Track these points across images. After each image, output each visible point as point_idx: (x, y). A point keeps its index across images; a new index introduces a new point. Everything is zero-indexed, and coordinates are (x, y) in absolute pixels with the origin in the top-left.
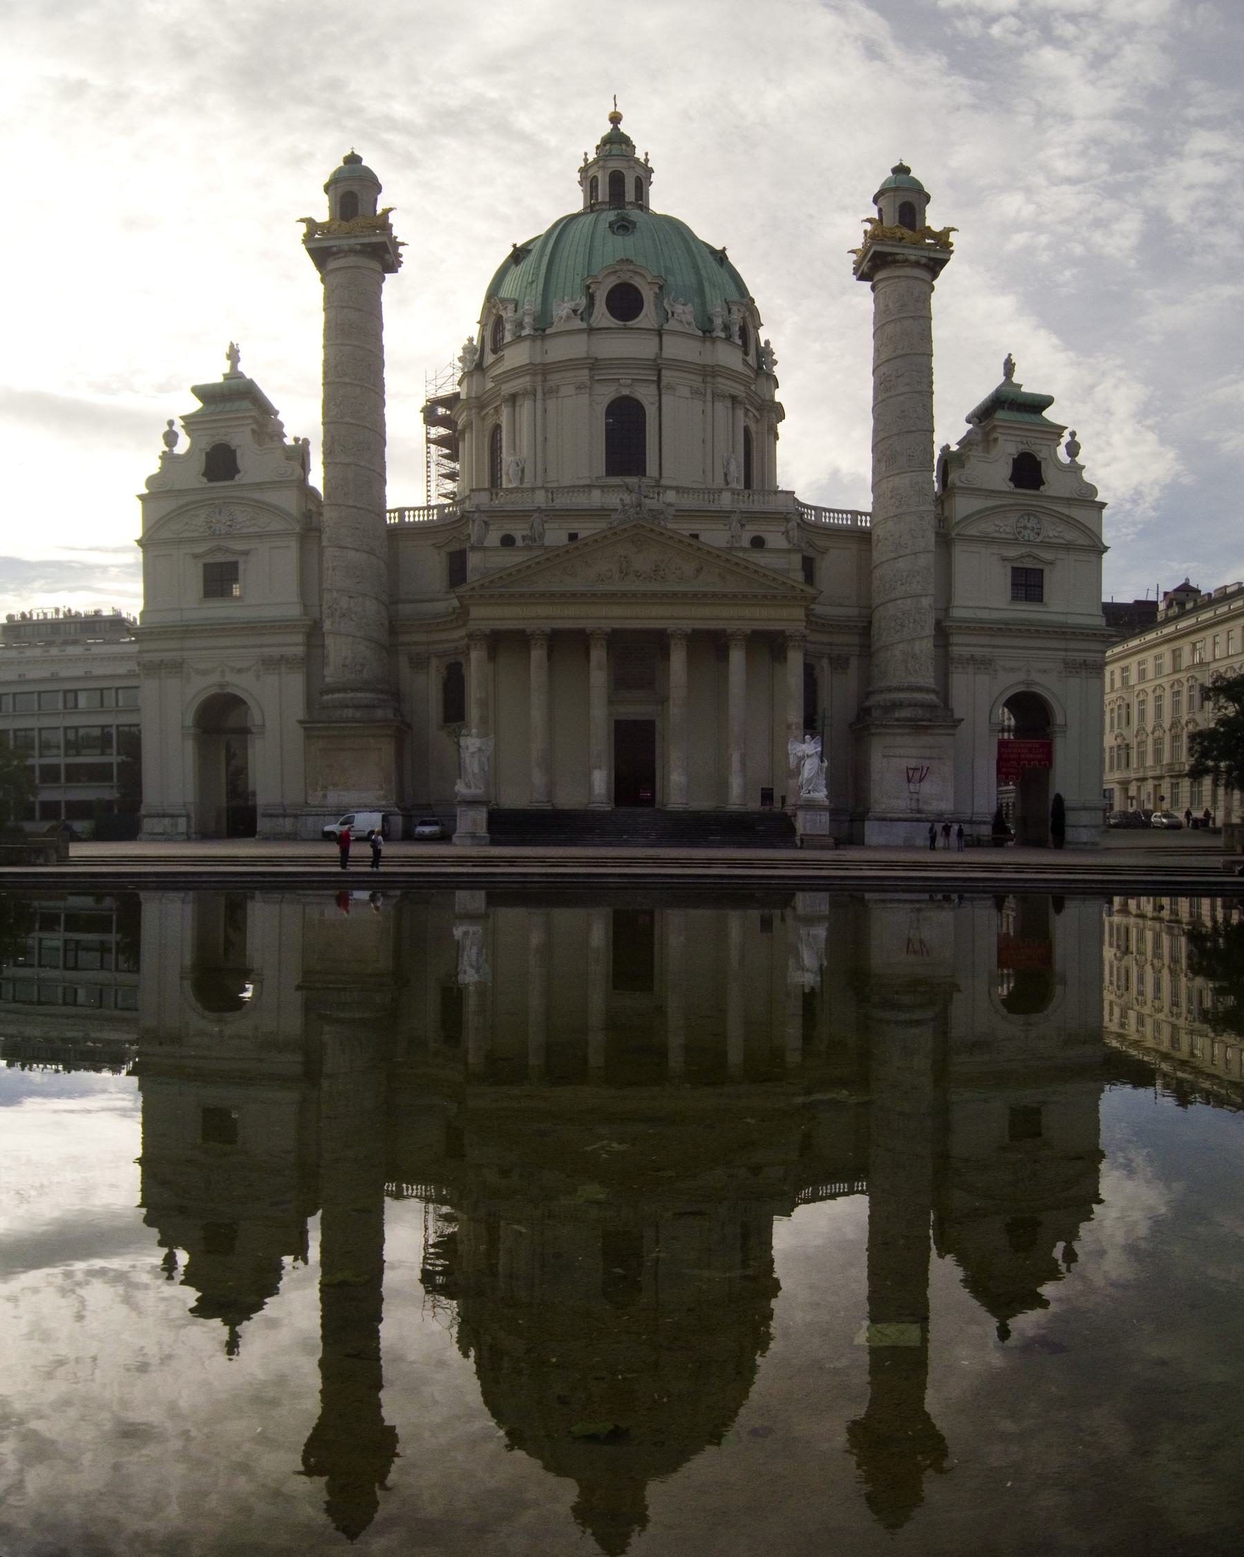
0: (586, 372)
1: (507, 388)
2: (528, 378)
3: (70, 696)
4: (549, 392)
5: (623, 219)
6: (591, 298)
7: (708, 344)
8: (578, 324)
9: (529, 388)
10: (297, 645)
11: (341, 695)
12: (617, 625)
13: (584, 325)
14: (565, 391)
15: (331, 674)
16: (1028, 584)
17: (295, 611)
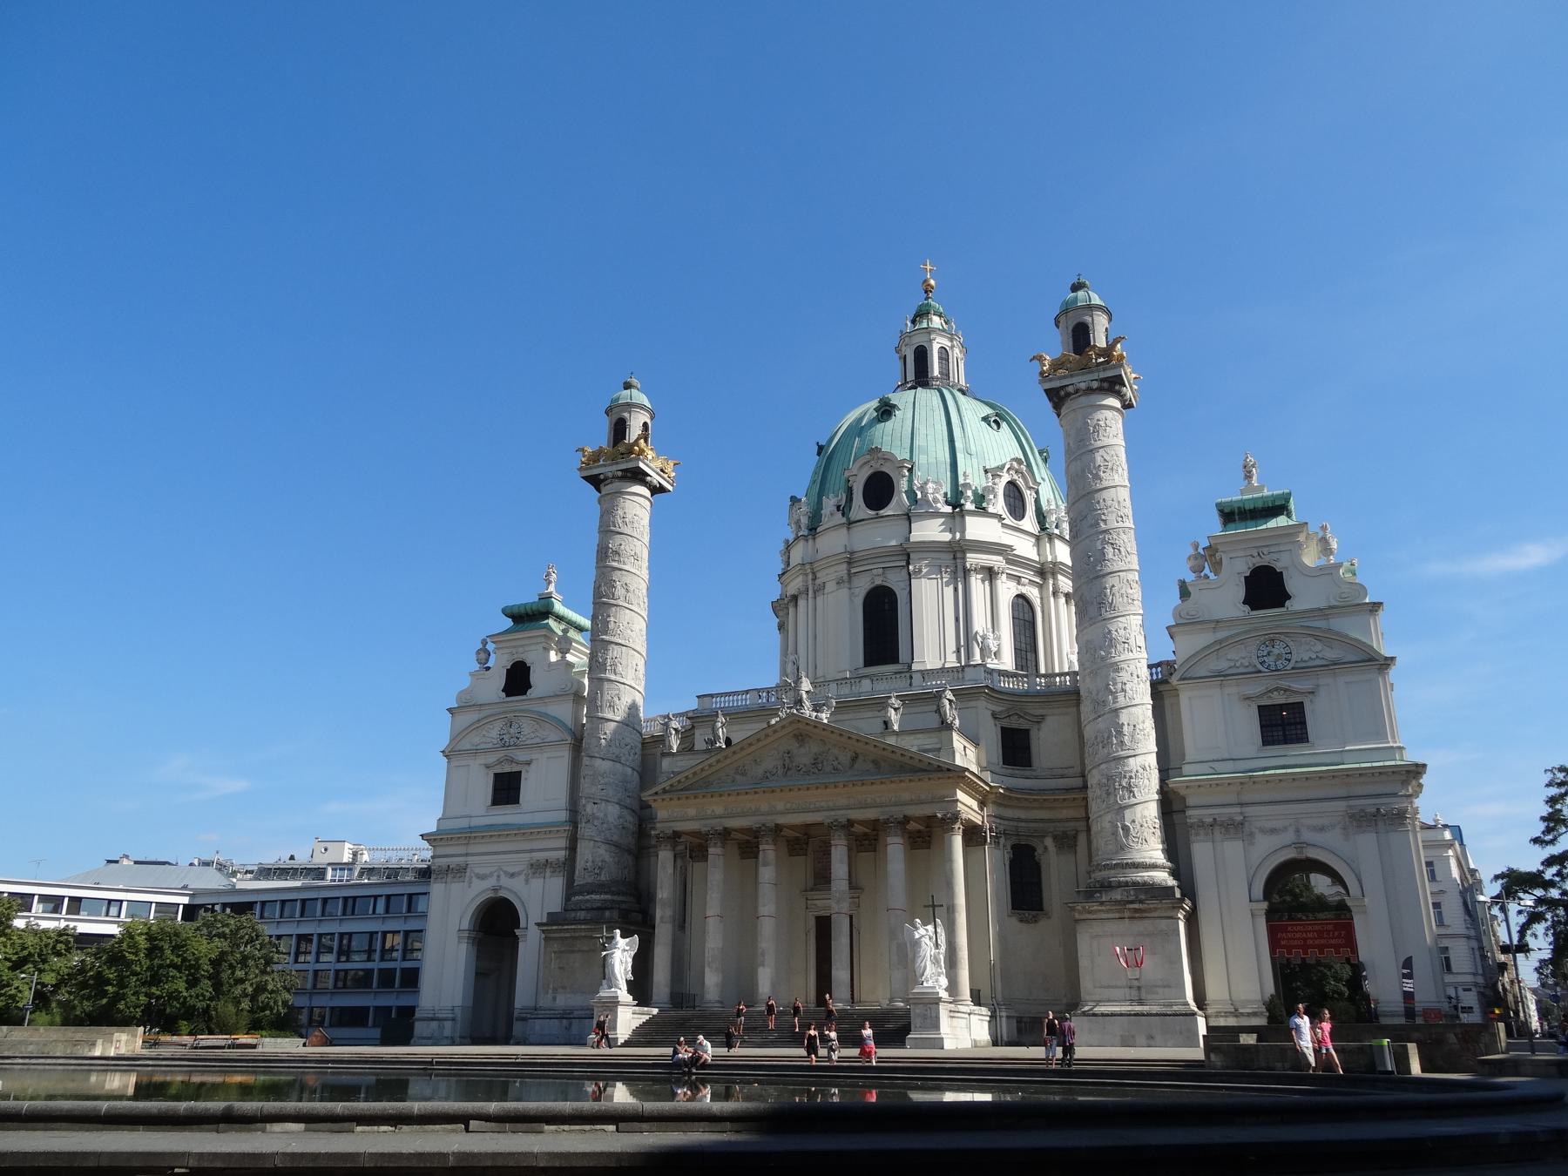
0: (845, 566)
1: (792, 590)
3: (350, 902)
4: (819, 589)
6: (850, 491)
7: (958, 519)
8: (839, 518)
12: (781, 820)
13: (844, 520)
15: (581, 878)
16: (1283, 724)
17: (563, 816)
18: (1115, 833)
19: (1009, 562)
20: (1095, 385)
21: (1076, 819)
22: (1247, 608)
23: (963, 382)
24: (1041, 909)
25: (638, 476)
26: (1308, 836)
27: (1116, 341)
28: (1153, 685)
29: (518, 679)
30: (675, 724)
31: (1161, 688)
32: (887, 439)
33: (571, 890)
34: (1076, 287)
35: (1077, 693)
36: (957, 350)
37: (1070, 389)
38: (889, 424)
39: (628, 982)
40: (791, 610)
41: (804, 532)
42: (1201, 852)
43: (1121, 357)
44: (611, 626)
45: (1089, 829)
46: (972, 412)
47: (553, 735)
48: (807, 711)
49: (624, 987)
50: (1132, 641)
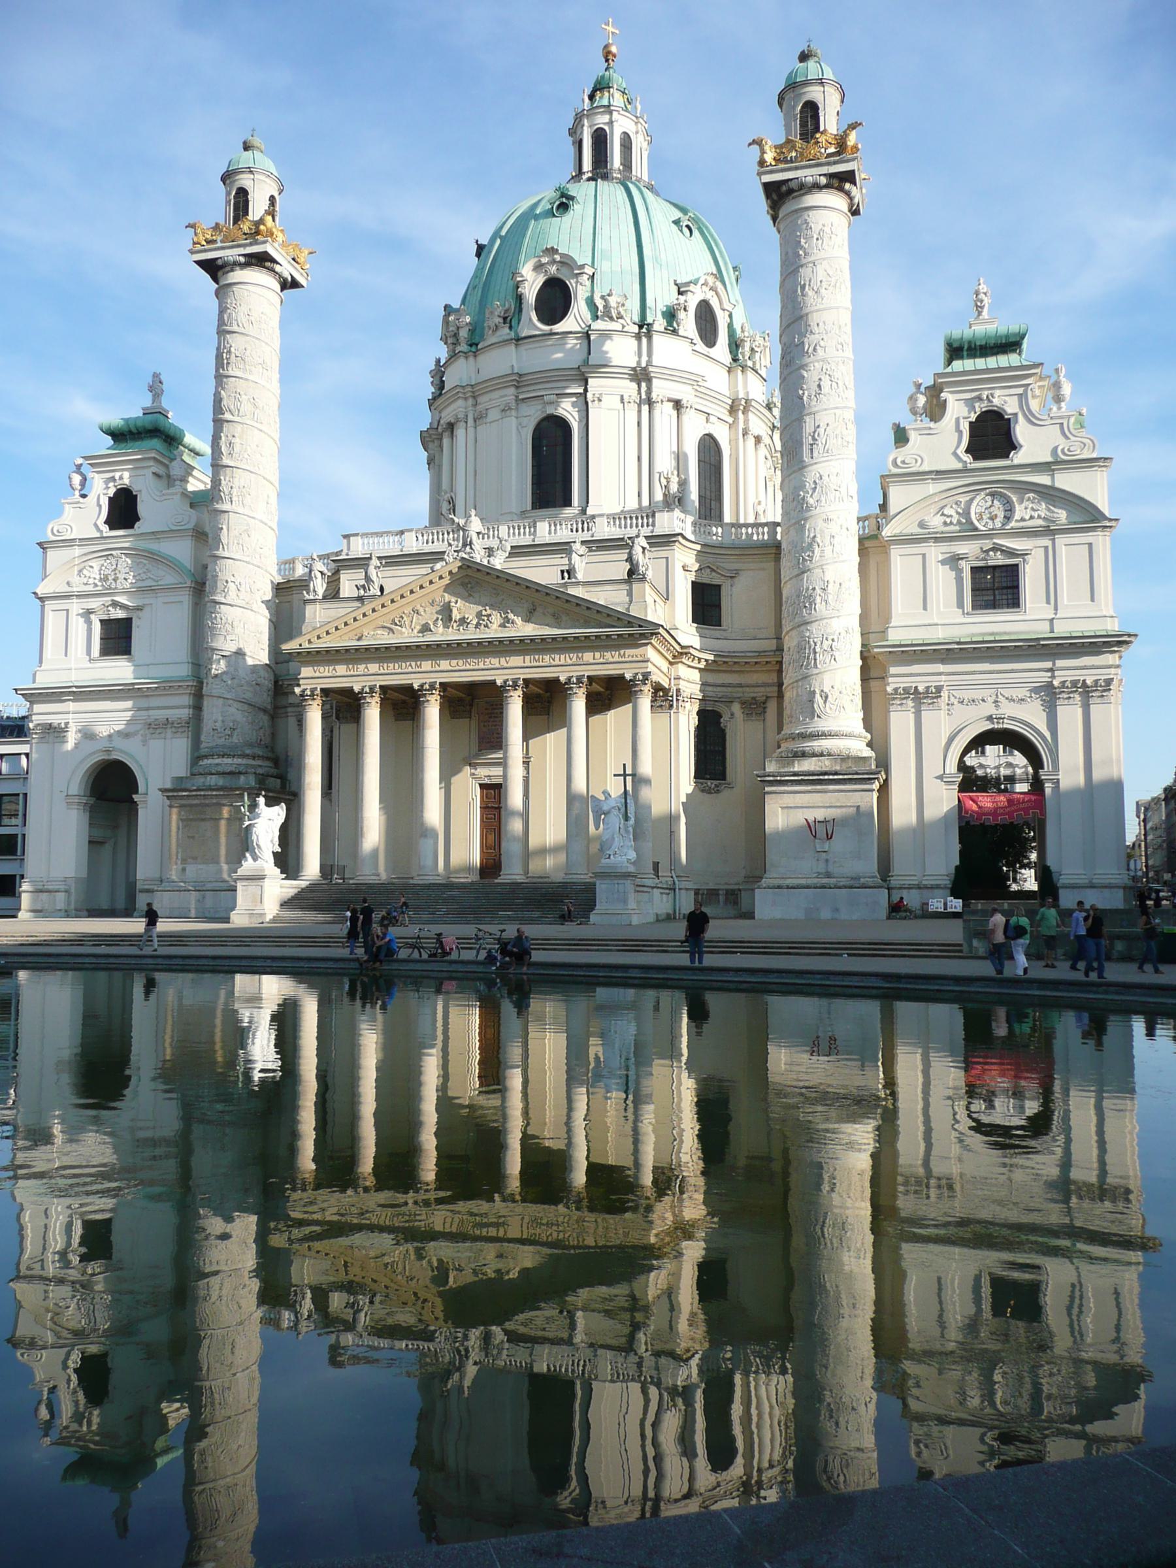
0: (512, 390)
1: (447, 416)
2: (460, 402)
5: (563, 195)
8: (505, 332)
9: (461, 416)
10: (184, 707)
11: (210, 761)
14: (493, 415)
17: (184, 670)
18: (812, 701)
19: (699, 394)
20: (823, 180)
21: (765, 685)
22: (968, 458)
23: (645, 177)
24: (724, 778)
25: (262, 260)
26: (1007, 709)
27: (853, 126)
28: (861, 540)
29: (123, 509)
30: (319, 566)
31: (868, 544)
32: (564, 237)
33: (196, 757)
34: (804, 57)
35: (778, 546)
36: (641, 137)
37: (793, 185)
38: (567, 219)
39: (275, 854)
40: (446, 441)
41: (463, 347)
42: (901, 722)
43: (855, 149)
44: (237, 448)
45: (780, 696)
46: (660, 215)
47: (169, 579)
48: (479, 556)
49: (271, 860)
50: (843, 490)
